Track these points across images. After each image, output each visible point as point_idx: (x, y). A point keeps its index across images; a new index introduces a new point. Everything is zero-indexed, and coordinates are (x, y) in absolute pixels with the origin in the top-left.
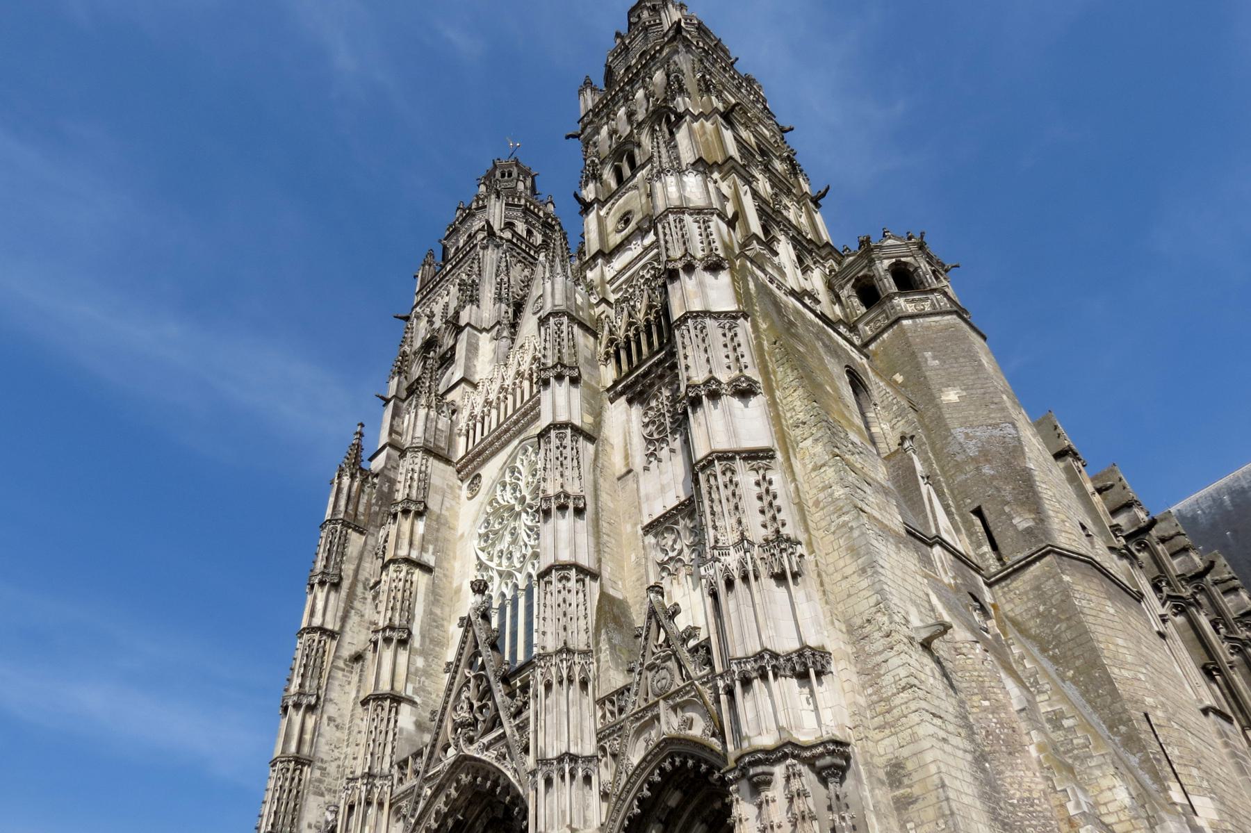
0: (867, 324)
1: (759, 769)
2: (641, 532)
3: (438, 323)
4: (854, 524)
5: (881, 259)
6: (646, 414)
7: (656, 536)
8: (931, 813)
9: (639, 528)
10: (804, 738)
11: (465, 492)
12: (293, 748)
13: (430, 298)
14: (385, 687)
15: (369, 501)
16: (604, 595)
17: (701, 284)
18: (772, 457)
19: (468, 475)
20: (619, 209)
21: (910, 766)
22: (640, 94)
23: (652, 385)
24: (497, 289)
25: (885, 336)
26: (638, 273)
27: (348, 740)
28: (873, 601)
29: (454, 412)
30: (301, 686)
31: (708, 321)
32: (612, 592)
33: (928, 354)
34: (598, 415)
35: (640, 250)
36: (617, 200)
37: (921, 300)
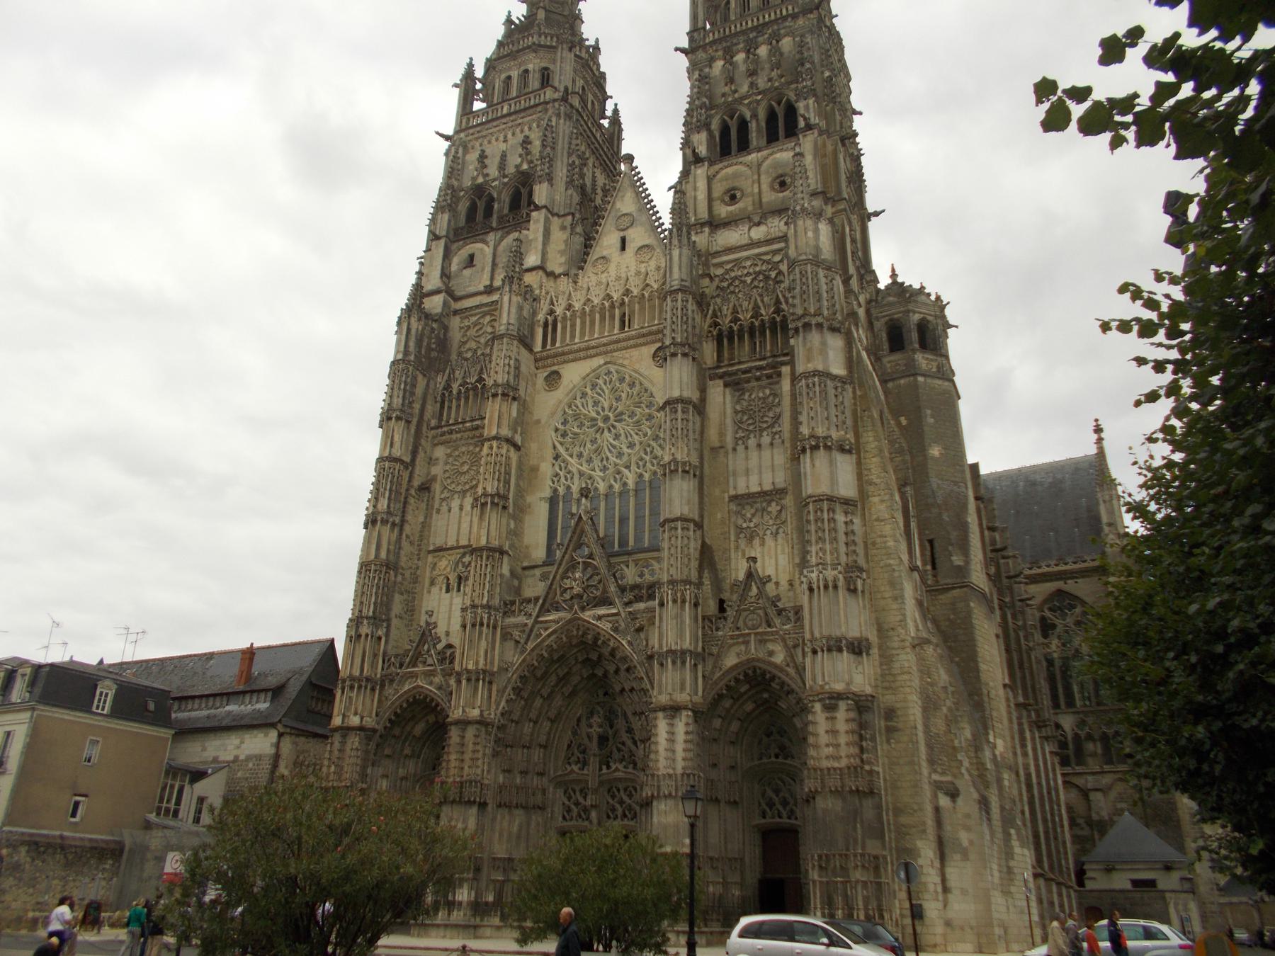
0: (889, 362)
1: (833, 702)
2: (727, 499)
3: (493, 171)
4: (896, 568)
5: (914, 312)
6: (738, 402)
7: (739, 505)
8: (905, 739)
9: (726, 496)
10: (854, 689)
11: (540, 381)
12: (383, 555)
14: (495, 543)
15: (429, 344)
16: (704, 544)
17: (824, 344)
18: (856, 506)
19: (544, 367)
20: (726, 178)
21: (899, 713)
22: (763, 51)
23: (748, 381)
24: (568, 171)
25: (902, 381)
27: (418, 555)
28: (898, 618)
29: (534, 300)
30: (389, 506)
31: (829, 382)
32: (707, 541)
33: (929, 412)
34: (703, 390)
35: (746, 241)
36: (726, 167)
37: (932, 360)
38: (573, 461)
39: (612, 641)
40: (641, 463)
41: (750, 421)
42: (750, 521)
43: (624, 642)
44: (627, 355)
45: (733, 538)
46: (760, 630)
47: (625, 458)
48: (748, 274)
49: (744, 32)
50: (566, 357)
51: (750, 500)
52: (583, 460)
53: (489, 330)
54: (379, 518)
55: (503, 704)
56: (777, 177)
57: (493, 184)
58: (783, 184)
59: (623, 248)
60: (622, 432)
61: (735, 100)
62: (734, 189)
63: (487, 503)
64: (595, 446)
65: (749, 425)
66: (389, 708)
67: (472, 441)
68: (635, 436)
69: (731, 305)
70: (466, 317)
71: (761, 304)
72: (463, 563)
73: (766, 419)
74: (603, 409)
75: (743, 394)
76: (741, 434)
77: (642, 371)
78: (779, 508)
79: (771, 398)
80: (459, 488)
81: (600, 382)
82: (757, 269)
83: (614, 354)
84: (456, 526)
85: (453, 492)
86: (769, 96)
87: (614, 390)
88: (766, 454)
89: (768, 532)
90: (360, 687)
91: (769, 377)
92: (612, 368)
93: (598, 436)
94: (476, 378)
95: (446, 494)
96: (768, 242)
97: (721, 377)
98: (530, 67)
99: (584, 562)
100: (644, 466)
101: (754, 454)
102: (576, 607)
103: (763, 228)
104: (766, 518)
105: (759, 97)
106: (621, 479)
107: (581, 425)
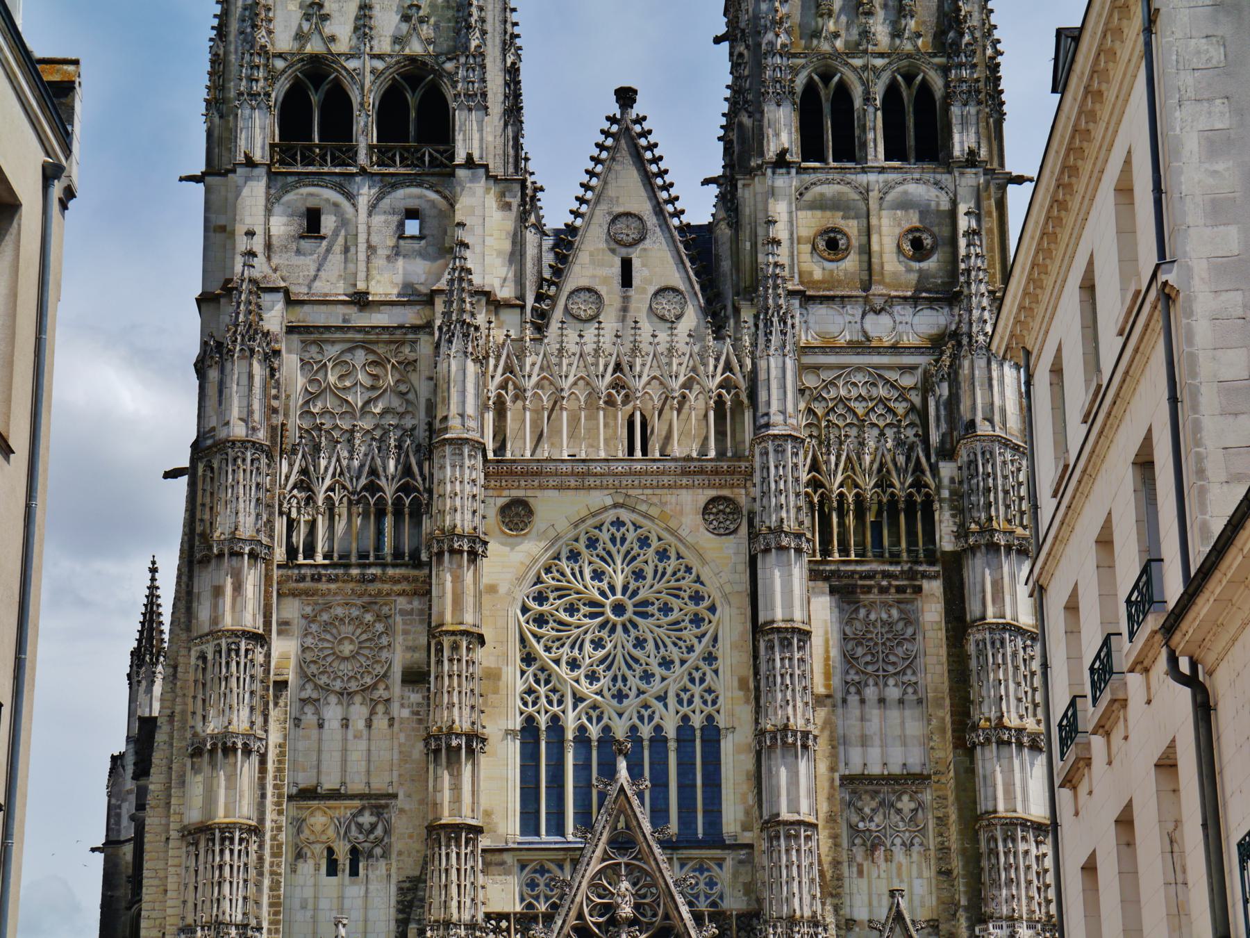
2: (837, 782)
3: (341, 29)
6: (850, 621)
7: (854, 792)
23: (868, 590)
26: (849, 374)
38: (563, 671)
40: (685, 697)
41: (868, 658)
42: (871, 820)
44: (655, 500)
45: (845, 844)
47: (656, 687)
48: (860, 398)
50: (544, 480)
51: (870, 787)
52: (581, 672)
54: (240, 745)
56: (911, 231)
57: (352, 64)
58: (917, 244)
59: (627, 280)
60: (649, 636)
61: (836, 54)
62: (833, 230)
63: (459, 747)
64: (600, 653)
65: (867, 663)
67: (359, 602)
68: (670, 646)
69: (843, 458)
70: (314, 342)
72: (360, 826)
73: (892, 658)
74: (612, 589)
75: (857, 610)
76: (852, 676)
77: (683, 533)
78: (913, 805)
79: (901, 624)
80: (338, 685)
81: (604, 536)
82: (874, 392)
83: (630, 492)
84: (337, 756)
85: (326, 689)
86: (894, 67)
87: (629, 558)
88: (894, 714)
89: (898, 841)
91: (900, 590)
92: (625, 515)
93: (604, 634)
94: (363, 481)
95: (309, 692)
96: (895, 349)
97: (825, 578)
99: (627, 865)
100: (690, 702)
101: (874, 713)
103: (885, 319)
104: (895, 818)
105: (879, 62)
106: (651, 718)
107: (571, 610)
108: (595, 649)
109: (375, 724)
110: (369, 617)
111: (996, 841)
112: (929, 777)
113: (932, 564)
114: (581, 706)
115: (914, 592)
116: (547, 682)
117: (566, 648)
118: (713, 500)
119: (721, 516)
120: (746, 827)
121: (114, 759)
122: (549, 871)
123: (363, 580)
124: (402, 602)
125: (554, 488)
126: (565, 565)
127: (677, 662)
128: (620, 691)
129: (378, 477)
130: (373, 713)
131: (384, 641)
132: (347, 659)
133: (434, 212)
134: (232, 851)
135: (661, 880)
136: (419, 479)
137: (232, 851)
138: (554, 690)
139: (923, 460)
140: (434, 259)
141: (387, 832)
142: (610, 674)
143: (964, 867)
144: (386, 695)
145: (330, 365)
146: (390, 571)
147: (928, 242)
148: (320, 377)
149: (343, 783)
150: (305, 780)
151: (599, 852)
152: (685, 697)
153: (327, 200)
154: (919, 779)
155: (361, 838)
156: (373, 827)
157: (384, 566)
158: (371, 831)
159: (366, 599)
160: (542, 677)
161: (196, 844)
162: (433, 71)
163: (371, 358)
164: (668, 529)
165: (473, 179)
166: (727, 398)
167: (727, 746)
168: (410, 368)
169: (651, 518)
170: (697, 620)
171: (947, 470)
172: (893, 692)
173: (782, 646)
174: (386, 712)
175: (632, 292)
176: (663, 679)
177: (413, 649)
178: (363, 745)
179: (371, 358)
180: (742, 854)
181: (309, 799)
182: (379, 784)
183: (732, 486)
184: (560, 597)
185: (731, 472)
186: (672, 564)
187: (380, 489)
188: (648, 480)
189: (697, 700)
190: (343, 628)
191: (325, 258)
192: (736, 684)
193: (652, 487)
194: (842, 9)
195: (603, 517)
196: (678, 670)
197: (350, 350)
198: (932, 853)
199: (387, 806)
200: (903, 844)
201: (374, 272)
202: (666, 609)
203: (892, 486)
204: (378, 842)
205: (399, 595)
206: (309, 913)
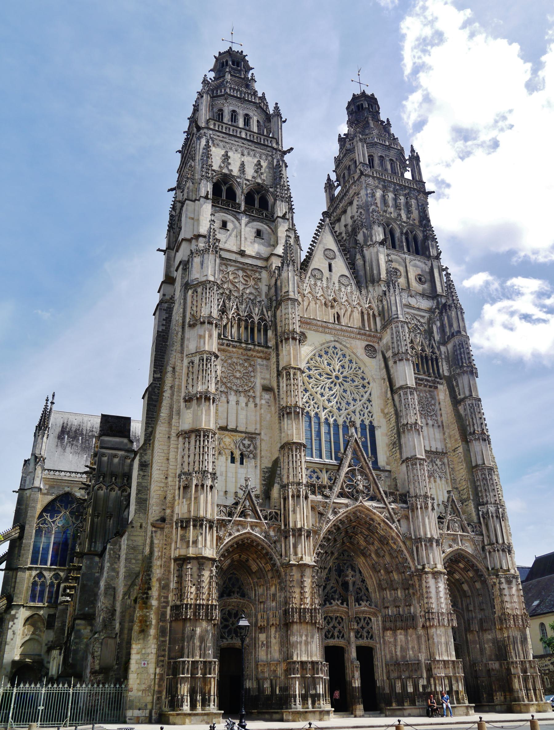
13: (225, 138)
23: (421, 386)
39: (382, 524)
40: (362, 413)
43: (393, 526)
44: (348, 342)
46: (460, 533)
47: (352, 408)
49: (395, 184)
53: (244, 282)
54: (212, 398)
55: (315, 554)
56: (419, 275)
58: (420, 279)
59: (330, 270)
64: (332, 393)
66: (225, 545)
67: (243, 358)
68: (356, 394)
70: (224, 264)
71: (424, 344)
72: (244, 445)
73: (429, 410)
77: (358, 355)
78: (441, 463)
80: (235, 388)
81: (330, 351)
82: (413, 322)
85: (231, 388)
86: (408, 227)
88: (431, 430)
89: (438, 476)
90: (211, 527)
91: (430, 387)
92: (337, 345)
93: (332, 385)
94: (246, 314)
98: (251, 114)
100: (364, 415)
102: (361, 498)
103: (414, 299)
104: (435, 467)
105: (404, 224)
107: (320, 375)
108: (329, 391)
109: (249, 405)
110: (246, 364)
111: (485, 474)
112: (446, 453)
113: (441, 379)
114: (326, 411)
115: (434, 388)
116: (313, 400)
117: (319, 388)
118: (367, 345)
119: (370, 352)
120: (388, 464)
121: (25, 461)
122: (317, 473)
123: (246, 349)
124: (259, 361)
125: (314, 330)
126: (318, 359)
127: (358, 400)
128: (339, 407)
129: (251, 313)
130: (249, 401)
131: (252, 374)
132: (237, 378)
133: (266, 232)
134: (208, 441)
135: (371, 477)
136: (267, 317)
137: (208, 441)
138: (316, 403)
139: (434, 345)
140: (267, 247)
141: (255, 448)
142: (336, 400)
143: (470, 485)
144: (253, 395)
145: (230, 273)
146: (257, 348)
147: (423, 279)
148: (226, 276)
149: (237, 427)
150: (223, 423)
151: (347, 464)
152: (362, 413)
153: (230, 219)
154: (444, 454)
155: (244, 449)
156: (249, 445)
157: (255, 345)
158: (249, 448)
159: (246, 357)
160: (311, 398)
161: (189, 438)
162: (265, 190)
163: (245, 274)
164: (353, 352)
165: (284, 222)
166: (371, 312)
167: (378, 434)
168: (259, 281)
169: (347, 348)
170: (364, 387)
171: (443, 349)
172: (430, 422)
173: (411, 394)
174: (254, 401)
175: (332, 274)
176: (354, 406)
177: (264, 379)
178: (244, 413)
179: (245, 274)
180: (387, 474)
181: (224, 430)
182: (251, 429)
183: (373, 342)
184: (316, 370)
185: (374, 337)
186: (354, 366)
187: (252, 317)
188: (346, 334)
189: (366, 415)
190: (236, 367)
191: (229, 237)
192: (380, 410)
193: (347, 337)
194: (392, 207)
195: (330, 344)
196: (359, 403)
197: (237, 270)
198: (449, 481)
199: (255, 438)
200: (440, 477)
201: (246, 246)
202: (353, 381)
203: (425, 351)
204: (251, 452)
205: (259, 358)
206: (224, 478)
